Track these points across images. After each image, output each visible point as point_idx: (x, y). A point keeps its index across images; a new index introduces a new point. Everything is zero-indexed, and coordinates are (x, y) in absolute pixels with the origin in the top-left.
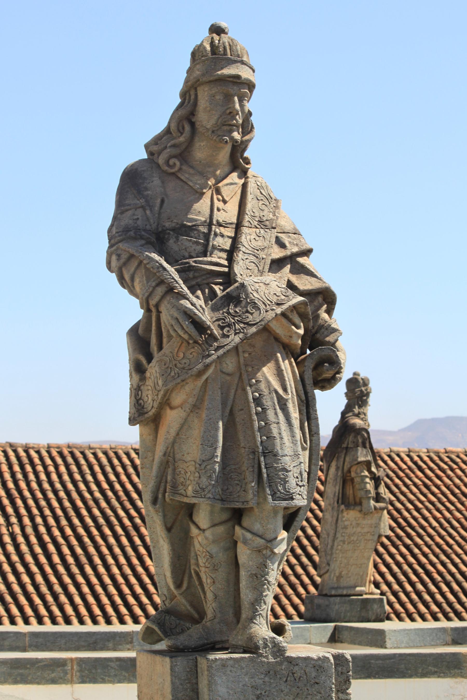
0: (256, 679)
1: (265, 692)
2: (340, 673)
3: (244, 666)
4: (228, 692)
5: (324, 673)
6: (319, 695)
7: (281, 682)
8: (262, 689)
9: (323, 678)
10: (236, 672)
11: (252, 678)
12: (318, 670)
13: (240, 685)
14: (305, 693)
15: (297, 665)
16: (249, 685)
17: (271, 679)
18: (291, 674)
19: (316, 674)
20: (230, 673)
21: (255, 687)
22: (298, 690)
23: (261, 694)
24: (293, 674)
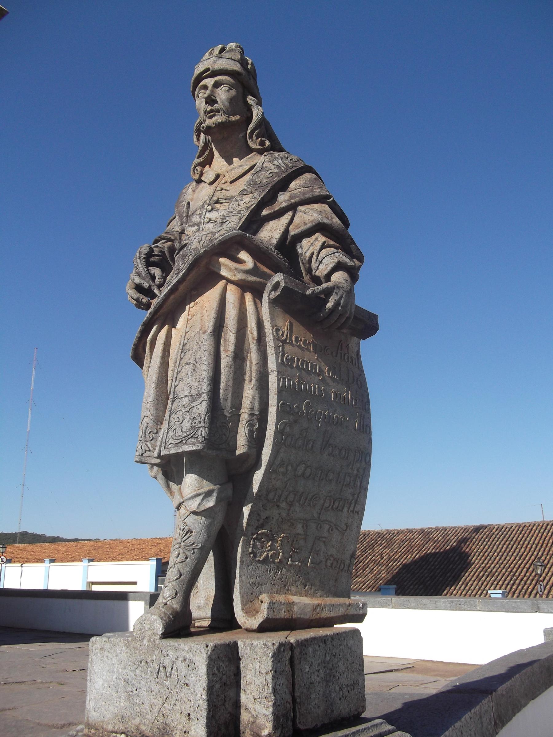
0: (128, 671)
1: (136, 690)
2: (257, 673)
3: (119, 652)
4: (103, 685)
5: (194, 671)
6: (188, 702)
7: (151, 678)
8: (133, 686)
9: (193, 678)
10: (111, 659)
11: (125, 669)
12: (189, 666)
13: (114, 677)
14: (174, 698)
15: (168, 655)
16: (122, 678)
17: (142, 672)
18: (161, 669)
19: (186, 672)
20: (107, 660)
21: (127, 682)
22: (168, 691)
23: (132, 691)
24: (165, 667)
